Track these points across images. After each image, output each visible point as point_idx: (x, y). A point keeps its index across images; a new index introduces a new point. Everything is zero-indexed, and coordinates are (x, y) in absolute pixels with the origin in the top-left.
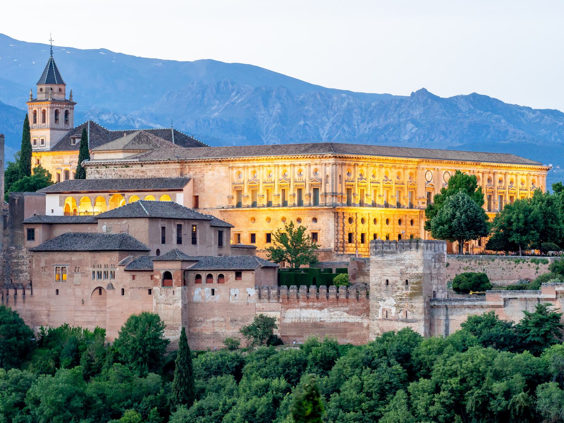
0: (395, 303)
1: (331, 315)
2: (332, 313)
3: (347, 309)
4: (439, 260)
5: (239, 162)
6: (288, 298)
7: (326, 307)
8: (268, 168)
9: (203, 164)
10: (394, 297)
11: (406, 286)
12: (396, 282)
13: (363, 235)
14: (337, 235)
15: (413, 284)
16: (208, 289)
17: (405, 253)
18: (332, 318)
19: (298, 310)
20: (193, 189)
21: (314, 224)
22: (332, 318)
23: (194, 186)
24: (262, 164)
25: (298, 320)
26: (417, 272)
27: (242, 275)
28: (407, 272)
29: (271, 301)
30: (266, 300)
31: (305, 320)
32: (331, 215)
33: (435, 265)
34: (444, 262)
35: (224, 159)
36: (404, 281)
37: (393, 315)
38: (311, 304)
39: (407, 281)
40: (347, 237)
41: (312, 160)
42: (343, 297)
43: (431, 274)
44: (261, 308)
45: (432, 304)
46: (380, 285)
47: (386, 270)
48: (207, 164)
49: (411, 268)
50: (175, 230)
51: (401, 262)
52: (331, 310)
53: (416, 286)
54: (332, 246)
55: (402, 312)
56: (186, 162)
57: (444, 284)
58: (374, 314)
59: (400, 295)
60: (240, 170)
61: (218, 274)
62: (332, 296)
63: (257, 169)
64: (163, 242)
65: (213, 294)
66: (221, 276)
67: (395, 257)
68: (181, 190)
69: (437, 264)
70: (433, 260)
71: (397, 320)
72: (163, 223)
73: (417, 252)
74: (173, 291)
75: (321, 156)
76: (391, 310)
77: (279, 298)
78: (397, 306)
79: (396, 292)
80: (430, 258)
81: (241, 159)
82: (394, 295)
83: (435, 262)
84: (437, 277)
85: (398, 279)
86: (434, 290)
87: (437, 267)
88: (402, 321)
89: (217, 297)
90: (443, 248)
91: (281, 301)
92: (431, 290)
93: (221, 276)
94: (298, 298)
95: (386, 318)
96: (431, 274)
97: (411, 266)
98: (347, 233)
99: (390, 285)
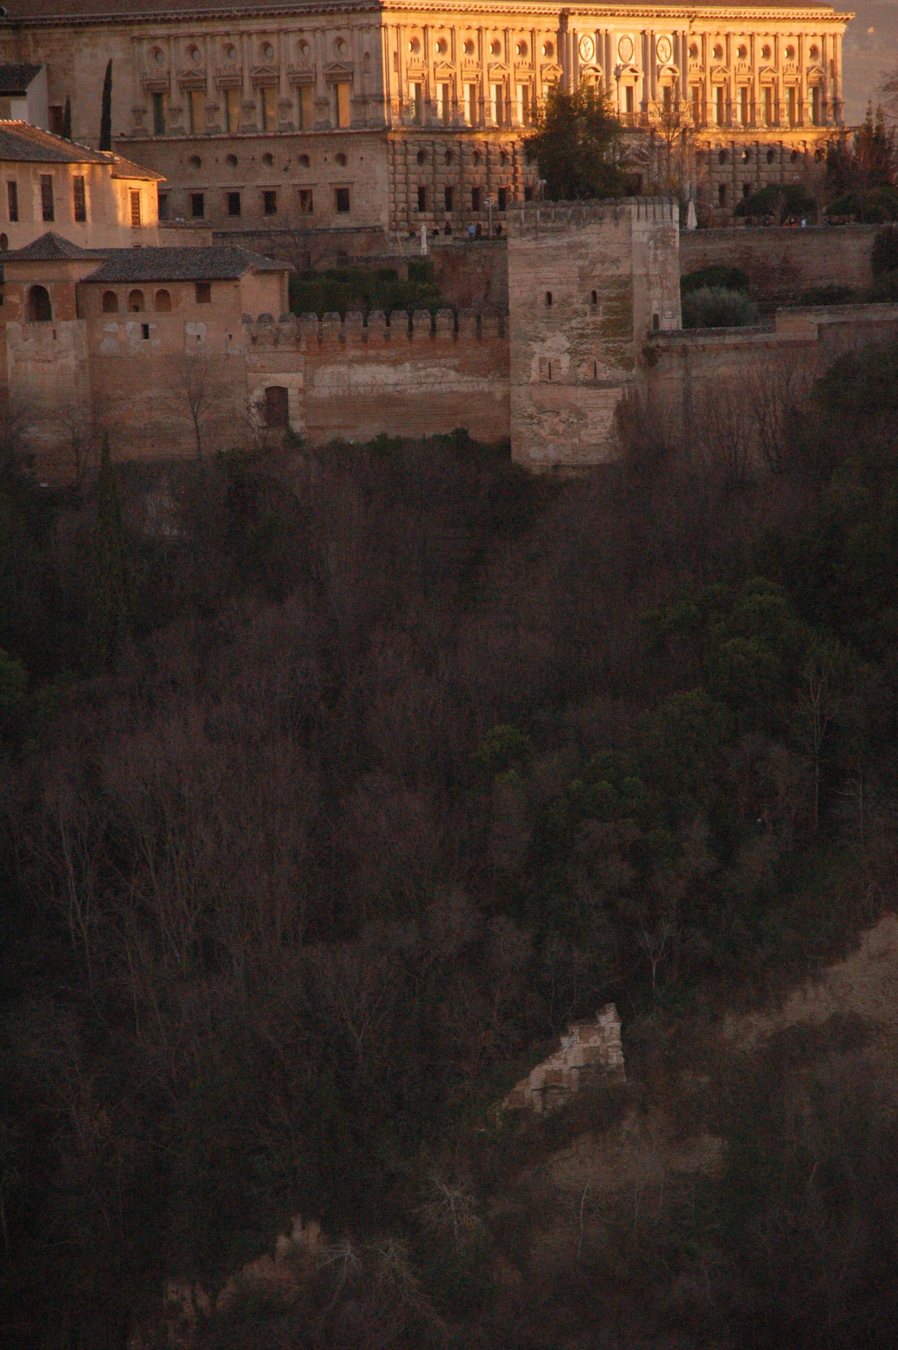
0: (568, 345)
1: (419, 376)
2: (423, 373)
3: (456, 361)
4: (663, 243)
5: (155, 26)
6: (320, 341)
7: (407, 360)
8: (226, 40)
9: (68, 30)
10: (565, 331)
11: (595, 305)
12: (570, 296)
13: (449, 191)
14: (394, 193)
15: (610, 299)
16: (132, 325)
17: (589, 229)
18: (420, 384)
19: (343, 369)
20: (49, 91)
21: (339, 168)
22: (420, 384)
23: (50, 83)
24: (209, 29)
25: (344, 392)
26: (618, 272)
27: (212, 290)
28: (595, 273)
29: (281, 348)
30: (269, 348)
31: (361, 390)
32: (379, 146)
33: (655, 255)
34: (674, 247)
35: (119, 19)
36: (588, 294)
37: (565, 371)
38: (372, 352)
39: (594, 293)
40: (415, 197)
41: (329, 18)
42: (445, 335)
43: (647, 275)
44: (259, 365)
45: (653, 343)
46: (532, 305)
47: (546, 272)
48: (77, 29)
49: (603, 263)
50: (36, 189)
51: (579, 251)
52: (420, 365)
53: (615, 304)
54: (384, 218)
55: (584, 364)
56: (27, 27)
57: (676, 296)
58: (521, 373)
59: (582, 325)
60: (159, 43)
61: (156, 290)
62: (420, 334)
63: (198, 43)
64: (14, 217)
65: (146, 335)
66: (163, 294)
67: (567, 239)
68: (23, 94)
69: (659, 252)
70: (652, 242)
71: (573, 385)
72: (11, 172)
73: (617, 225)
74: (54, 332)
75: (351, 8)
76: (559, 361)
77: (298, 340)
78: (572, 352)
79: (569, 319)
80: (644, 239)
81: (159, 18)
82: (565, 328)
83: (656, 248)
84: (661, 282)
85: (574, 289)
86: (655, 311)
87: (660, 258)
88: (587, 384)
89: (155, 341)
90: (671, 215)
91: (303, 347)
92: (649, 313)
93: (163, 294)
94: (342, 339)
95: (549, 379)
96: (647, 275)
97: (604, 259)
98: (414, 188)
99: (555, 305)
